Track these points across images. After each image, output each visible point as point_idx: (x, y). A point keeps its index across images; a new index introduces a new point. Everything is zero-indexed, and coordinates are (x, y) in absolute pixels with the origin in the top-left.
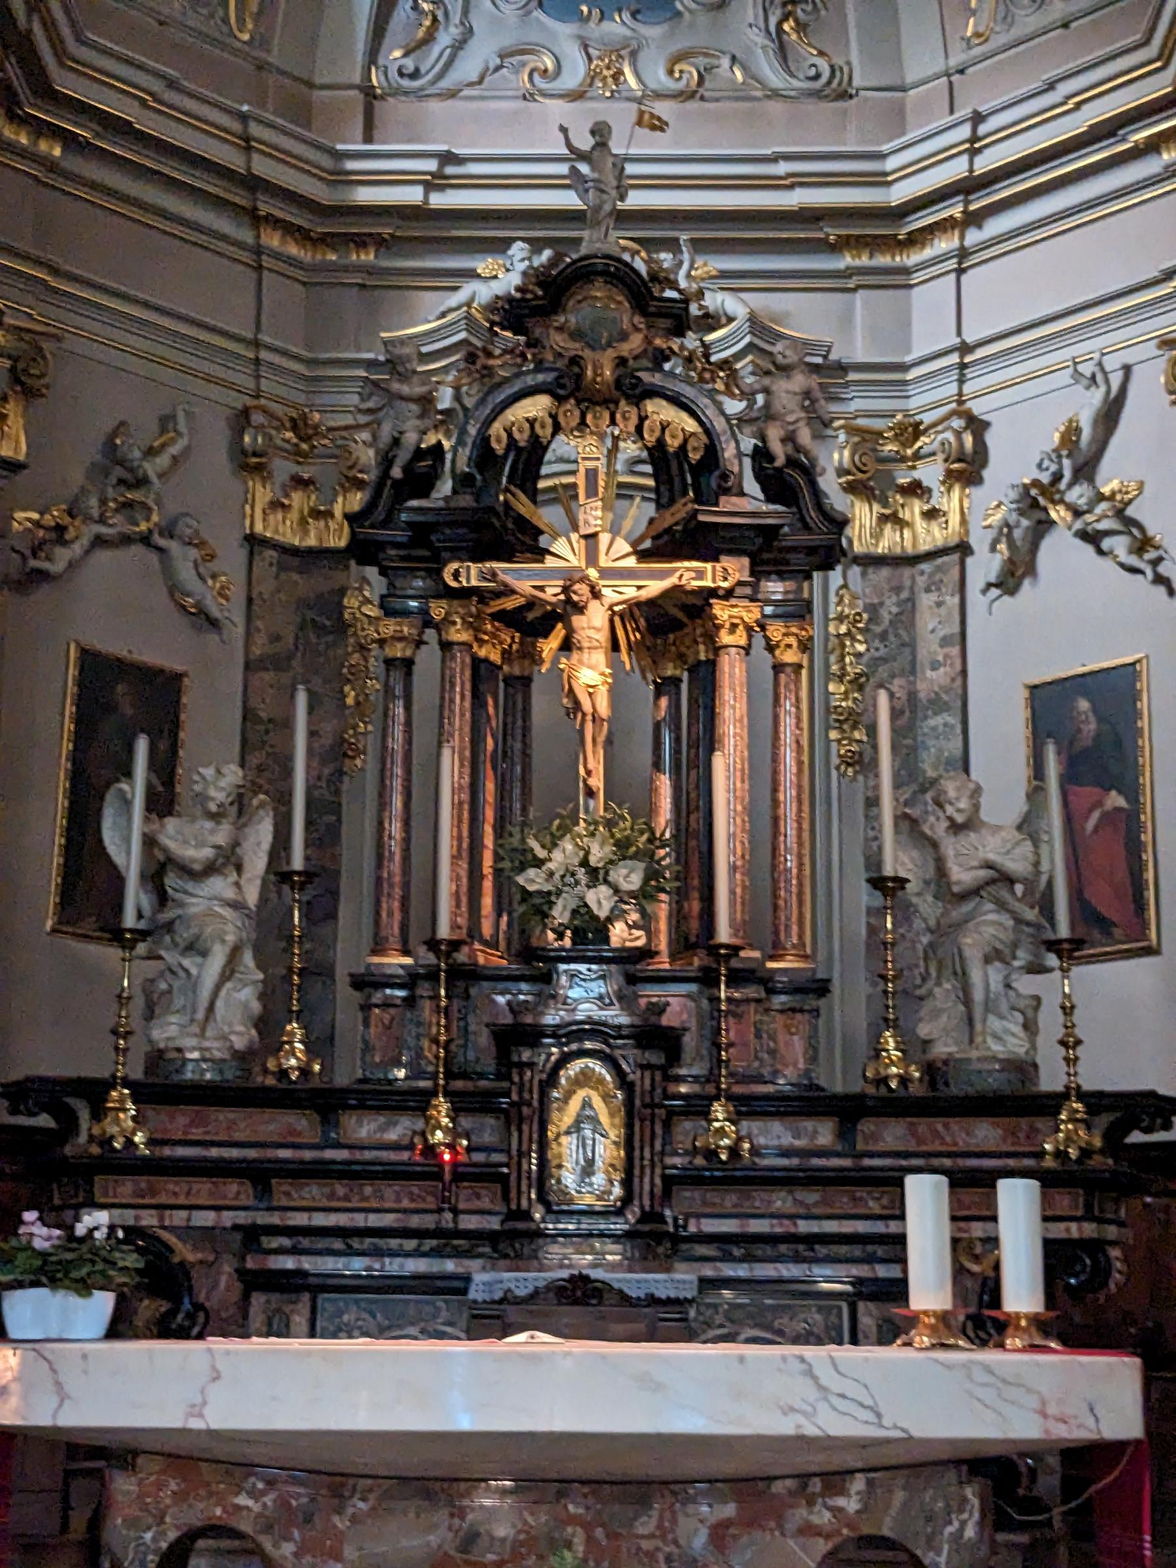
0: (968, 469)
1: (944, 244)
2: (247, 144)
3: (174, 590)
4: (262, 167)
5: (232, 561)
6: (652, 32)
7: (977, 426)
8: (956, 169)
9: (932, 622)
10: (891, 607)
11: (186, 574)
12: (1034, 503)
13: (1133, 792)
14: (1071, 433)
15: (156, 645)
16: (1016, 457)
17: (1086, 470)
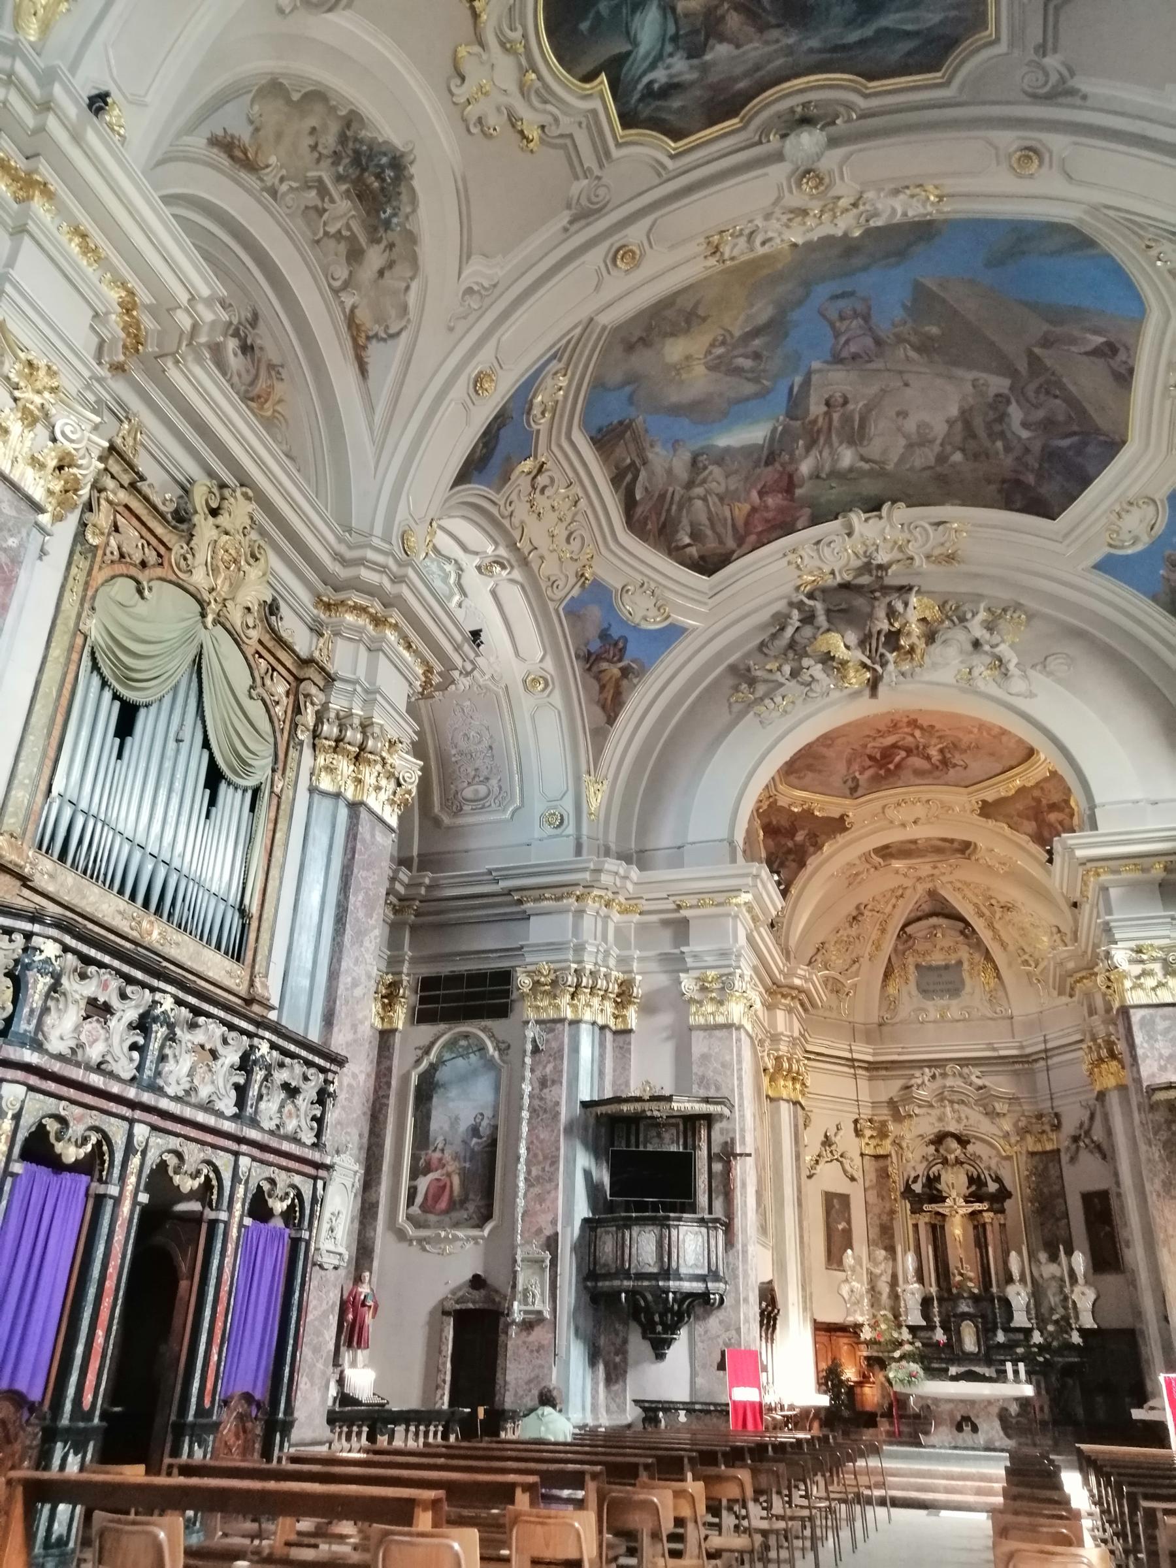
0: (1057, 1127)
1: (1042, 1063)
2: (851, 1051)
3: (845, 1171)
4: (856, 1056)
5: (858, 1160)
6: (954, 1002)
7: (1057, 1115)
8: (1042, 1047)
9: (1053, 1172)
10: (1041, 1167)
11: (848, 1167)
12: (1076, 1139)
13: (1112, 1227)
14: (1082, 1125)
15: (841, 1186)
16: (1069, 1126)
17: (1088, 1133)
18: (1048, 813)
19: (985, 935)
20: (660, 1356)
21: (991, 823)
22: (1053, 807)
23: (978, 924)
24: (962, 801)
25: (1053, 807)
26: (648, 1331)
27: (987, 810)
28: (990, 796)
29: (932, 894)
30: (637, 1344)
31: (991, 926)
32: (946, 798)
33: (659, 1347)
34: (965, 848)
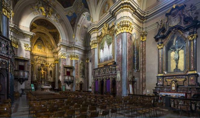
18: (56, 36)
19: (45, 44)
20: (21, 84)
21: (49, 34)
22: (56, 35)
23: (44, 42)
24: (48, 31)
25: (56, 35)
26: (20, 82)
27: (50, 32)
28: (51, 31)
29: (40, 37)
30: (19, 83)
31: (45, 43)
32: (47, 30)
33: (21, 84)
34: (45, 34)
